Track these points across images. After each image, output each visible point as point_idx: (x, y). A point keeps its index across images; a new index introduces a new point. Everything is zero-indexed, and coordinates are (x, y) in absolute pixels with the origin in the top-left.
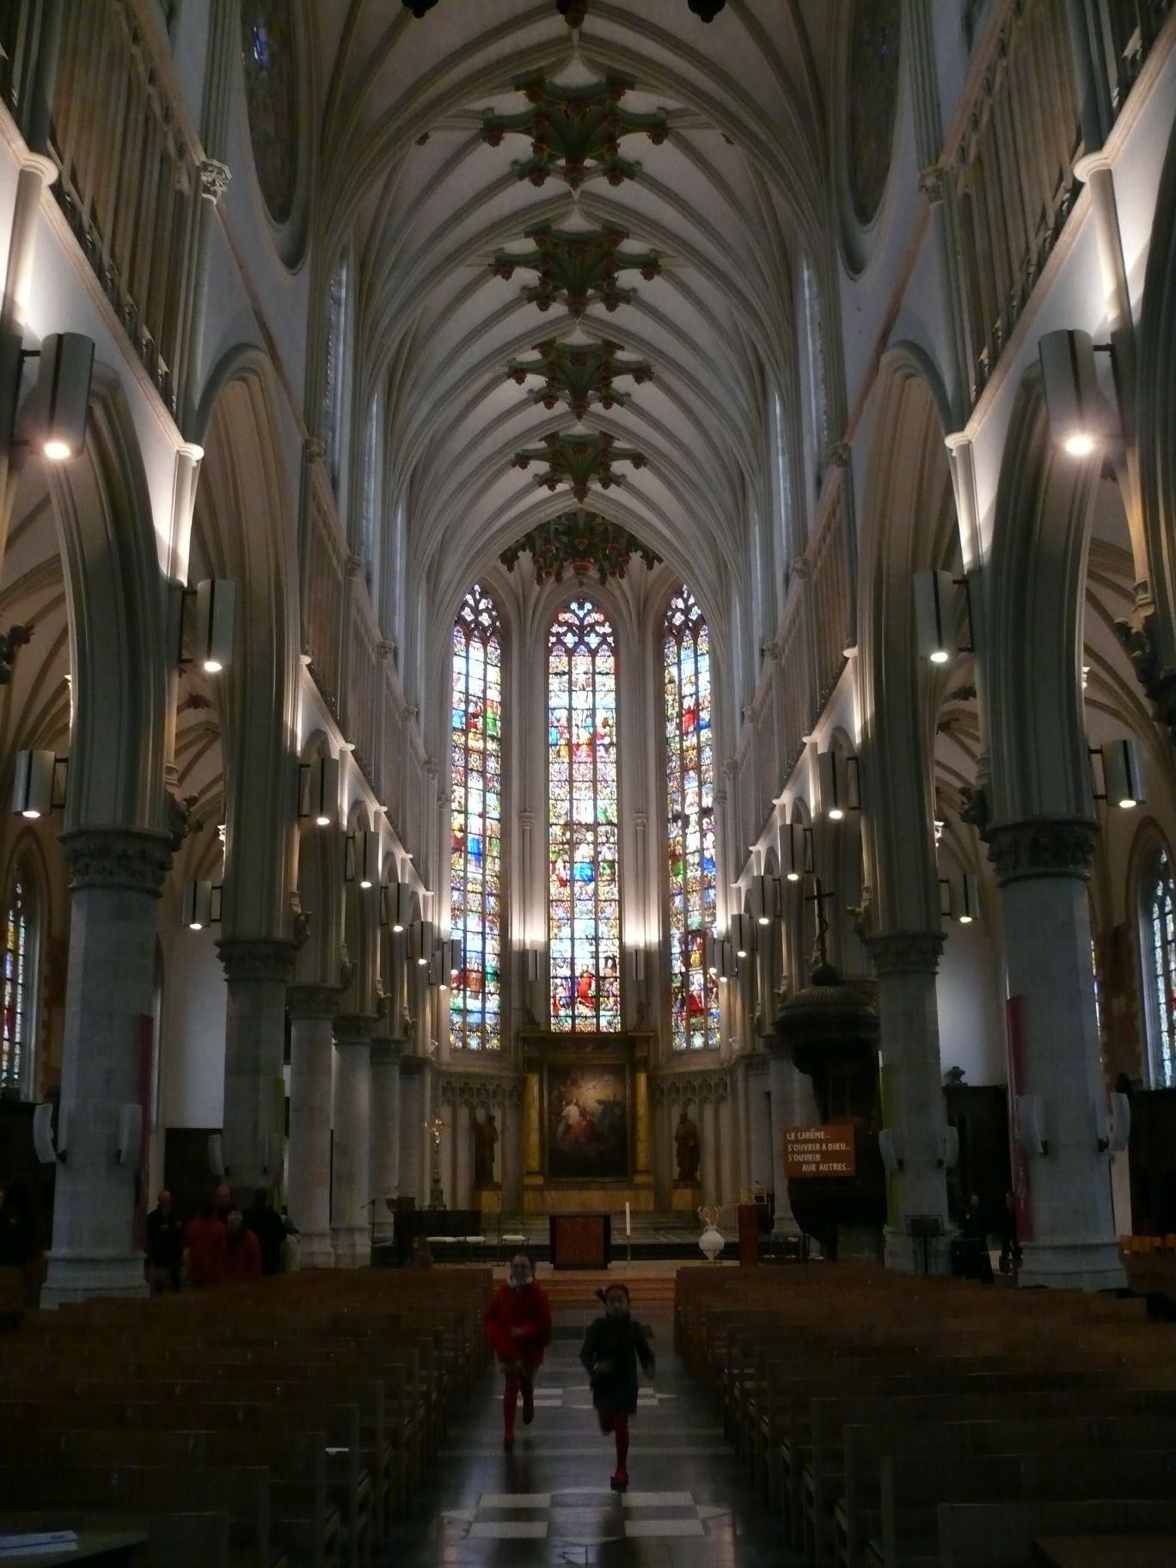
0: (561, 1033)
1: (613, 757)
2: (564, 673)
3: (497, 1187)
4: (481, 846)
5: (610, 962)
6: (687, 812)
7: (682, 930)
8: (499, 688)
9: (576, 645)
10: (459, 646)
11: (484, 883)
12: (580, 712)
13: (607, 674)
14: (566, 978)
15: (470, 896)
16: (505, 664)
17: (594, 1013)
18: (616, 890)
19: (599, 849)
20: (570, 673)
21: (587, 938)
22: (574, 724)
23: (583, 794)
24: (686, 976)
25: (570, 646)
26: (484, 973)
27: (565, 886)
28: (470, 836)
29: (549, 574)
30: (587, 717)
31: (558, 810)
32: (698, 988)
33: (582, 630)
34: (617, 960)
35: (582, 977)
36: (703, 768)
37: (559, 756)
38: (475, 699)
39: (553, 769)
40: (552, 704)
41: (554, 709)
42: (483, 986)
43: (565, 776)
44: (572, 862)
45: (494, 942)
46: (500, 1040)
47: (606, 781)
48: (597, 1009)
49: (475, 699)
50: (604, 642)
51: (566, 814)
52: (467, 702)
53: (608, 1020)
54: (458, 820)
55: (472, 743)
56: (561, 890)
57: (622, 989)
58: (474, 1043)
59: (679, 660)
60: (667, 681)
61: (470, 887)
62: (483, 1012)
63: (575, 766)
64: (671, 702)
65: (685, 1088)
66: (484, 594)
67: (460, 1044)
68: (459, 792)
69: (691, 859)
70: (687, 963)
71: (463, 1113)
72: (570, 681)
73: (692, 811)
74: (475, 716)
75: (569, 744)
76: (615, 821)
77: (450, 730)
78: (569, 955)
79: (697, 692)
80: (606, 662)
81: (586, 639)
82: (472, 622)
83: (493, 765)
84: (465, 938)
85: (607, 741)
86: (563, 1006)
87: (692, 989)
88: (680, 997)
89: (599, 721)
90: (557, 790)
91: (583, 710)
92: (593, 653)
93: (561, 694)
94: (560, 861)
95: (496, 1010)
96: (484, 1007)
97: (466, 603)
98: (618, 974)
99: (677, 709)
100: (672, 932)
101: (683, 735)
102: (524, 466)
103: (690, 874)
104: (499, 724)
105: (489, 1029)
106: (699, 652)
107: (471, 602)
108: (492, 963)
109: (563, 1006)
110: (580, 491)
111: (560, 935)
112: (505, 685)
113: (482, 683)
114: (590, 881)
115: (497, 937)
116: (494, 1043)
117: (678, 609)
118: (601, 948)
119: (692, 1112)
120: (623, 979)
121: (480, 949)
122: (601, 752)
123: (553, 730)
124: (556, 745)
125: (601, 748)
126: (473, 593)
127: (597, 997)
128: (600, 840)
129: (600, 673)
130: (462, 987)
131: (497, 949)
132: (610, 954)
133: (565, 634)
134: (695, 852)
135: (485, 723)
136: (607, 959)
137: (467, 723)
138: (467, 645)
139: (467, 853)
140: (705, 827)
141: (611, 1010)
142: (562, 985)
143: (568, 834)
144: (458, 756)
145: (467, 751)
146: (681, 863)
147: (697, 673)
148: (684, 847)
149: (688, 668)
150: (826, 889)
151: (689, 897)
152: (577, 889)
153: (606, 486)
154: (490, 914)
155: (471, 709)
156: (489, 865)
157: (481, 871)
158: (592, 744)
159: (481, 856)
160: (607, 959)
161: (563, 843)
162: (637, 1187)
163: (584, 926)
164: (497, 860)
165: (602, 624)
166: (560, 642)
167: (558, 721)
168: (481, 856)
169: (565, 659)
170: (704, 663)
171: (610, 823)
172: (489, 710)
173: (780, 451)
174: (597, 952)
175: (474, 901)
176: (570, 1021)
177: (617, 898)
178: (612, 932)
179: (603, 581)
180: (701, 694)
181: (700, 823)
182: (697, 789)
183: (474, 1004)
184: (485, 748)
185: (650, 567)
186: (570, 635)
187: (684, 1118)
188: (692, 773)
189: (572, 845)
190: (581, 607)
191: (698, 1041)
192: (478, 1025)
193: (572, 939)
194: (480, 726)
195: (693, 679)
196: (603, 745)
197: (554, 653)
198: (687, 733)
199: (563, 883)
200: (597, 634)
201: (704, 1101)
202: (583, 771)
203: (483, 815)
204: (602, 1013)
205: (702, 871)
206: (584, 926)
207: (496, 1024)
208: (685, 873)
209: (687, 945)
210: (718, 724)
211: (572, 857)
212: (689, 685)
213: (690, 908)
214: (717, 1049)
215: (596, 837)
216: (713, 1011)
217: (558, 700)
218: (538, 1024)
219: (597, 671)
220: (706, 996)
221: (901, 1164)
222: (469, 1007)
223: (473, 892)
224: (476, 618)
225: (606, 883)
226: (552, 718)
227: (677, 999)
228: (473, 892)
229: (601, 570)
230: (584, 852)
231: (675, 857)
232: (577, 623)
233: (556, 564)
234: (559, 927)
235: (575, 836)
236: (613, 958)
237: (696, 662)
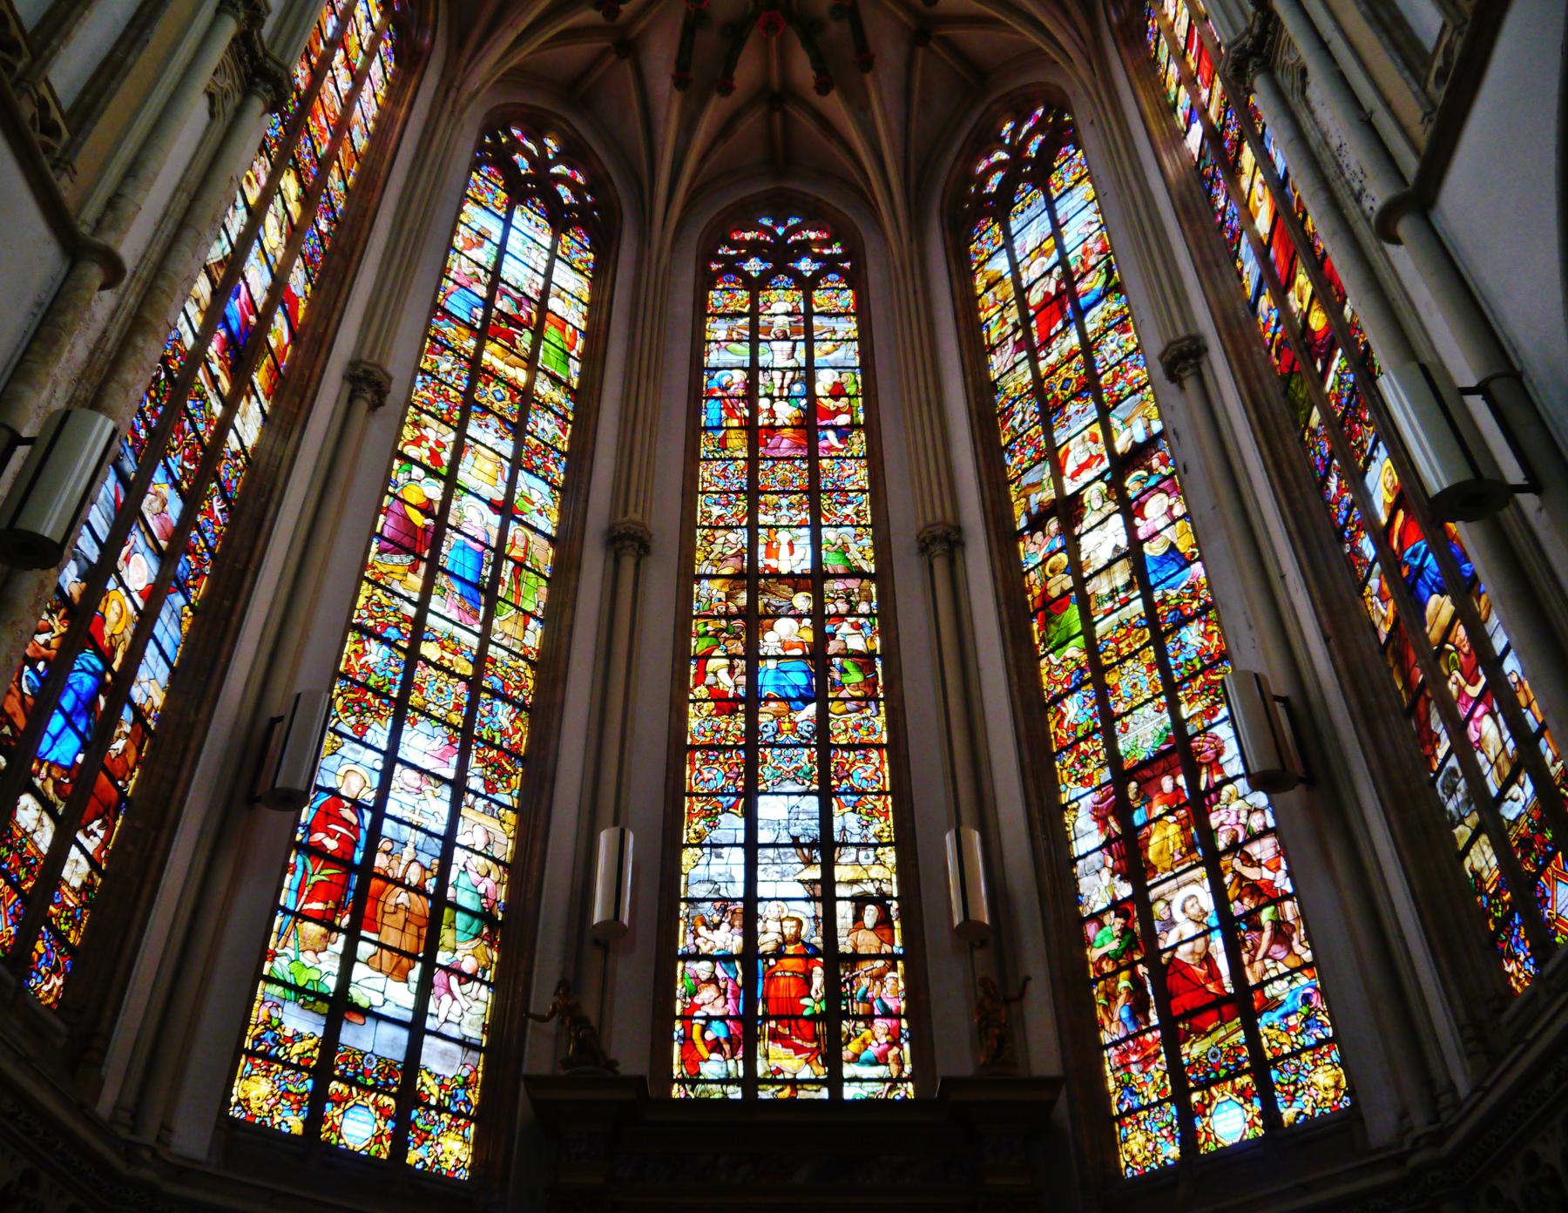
2: (741, 315)
4: (487, 572)
6: (1070, 488)
11: (481, 660)
14: (727, 959)
17: (822, 1072)
18: (880, 722)
19: (828, 629)
21: (796, 843)
26: (440, 901)
27: (733, 712)
30: (793, 382)
31: (717, 548)
32: (1190, 930)
34: (895, 905)
35: (779, 954)
37: (725, 448)
39: (707, 473)
40: (714, 358)
41: (717, 369)
42: (432, 944)
44: (753, 657)
45: (493, 824)
46: (479, 1145)
47: (844, 492)
48: (833, 1060)
51: (739, 554)
56: (722, 721)
57: (911, 994)
67: (294, 1123)
72: (754, 327)
75: (750, 426)
76: (870, 567)
78: (738, 890)
79: (1063, 255)
83: (545, 426)
85: (843, 420)
87: (1170, 939)
88: (1123, 982)
89: (821, 388)
91: (783, 370)
92: (807, 285)
93: (733, 346)
95: (474, 1033)
96: (421, 1011)
98: (898, 948)
100: (1064, 799)
103: (1100, 629)
105: (430, 1087)
109: (715, 1046)
111: (716, 836)
112: (598, 309)
113: (541, 280)
114: (806, 701)
115: (510, 817)
118: (840, 873)
120: (914, 960)
121: (439, 827)
124: (720, 428)
125: (831, 434)
127: (833, 1014)
128: (831, 609)
131: (504, 848)
132: (870, 888)
134: (1111, 563)
136: (860, 902)
139: (434, 568)
141: (880, 1060)
142: (713, 980)
143: (743, 598)
151: (1111, 679)
154: (490, 744)
155: (503, 304)
156: (505, 623)
157: (478, 628)
158: (809, 424)
159: (485, 595)
160: (860, 902)
161: (728, 616)
164: (533, 623)
167: (725, 388)
168: (485, 595)
171: (859, 574)
174: (828, 881)
178: (875, 828)
181: (1116, 488)
189: (754, 621)
192: (388, 1066)
194: (525, 339)
196: (835, 428)
200: (816, 258)
203: (506, 509)
204: (848, 1070)
207: (466, 1084)
216: (1276, 989)
220: (1233, 949)
223: (438, 667)
225: (851, 705)
226: (712, 383)
227: (1111, 997)
228: (438, 667)
230: (784, 633)
236: (881, 900)
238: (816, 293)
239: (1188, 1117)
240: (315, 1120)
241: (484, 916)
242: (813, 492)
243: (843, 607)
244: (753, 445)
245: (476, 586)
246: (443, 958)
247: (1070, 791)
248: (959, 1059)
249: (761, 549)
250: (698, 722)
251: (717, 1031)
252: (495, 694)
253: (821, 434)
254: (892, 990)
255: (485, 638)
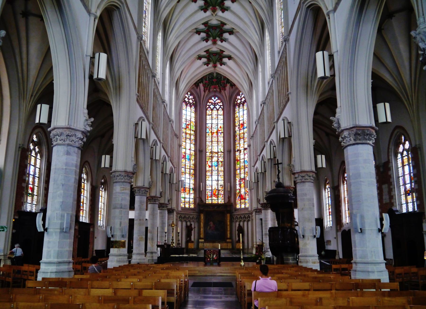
0: (209, 204)
1: (222, 136)
2: (210, 115)
3: (193, 242)
4: (189, 157)
5: (221, 186)
6: (241, 149)
7: (239, 178)
8: (194, 118)
9: (214, 108)
10: (184, 107)
11: (190, 166)
12: (214, 124)
13: (221, 115)
14: (210, 190)
15: (186, 169)
16: (196, 111)
17: (217, 199)
18: (223, 168)
20: (212, 115)
22: (213, 127)
23: (215, 144)
24: (240, 190)
25: (212, 108)
26: (190, 189)
27: (210, 167)
28: (187, 155)
29: (207, 89)
31: (209, 149)
33: (215, 104)
34: (223, 186)
35: (214, 190)
36: (245, 138)
38: (188, 121)
39: (207, 138)
40: (207, 122)
42: (190, 192)
43: (210, 140)
44: (212, 161)
47: (221, 142)
48: (218, 198)
49: (188, 121)
50: (220, 107)
51: (211, 150)
52: (186, 121)
53: (221, 201)
54: (183, 151)
55: (187, 132)
56: (209, 168)
57: (224, 193)
58: (187, 206)
59: (239, 112)
60: (236, 117)
61: (186, 167)
62: (189, 198)
63: (213, 138)
64: (237, 122)
65: (240, 218)
66: (191, 95)
68: (184, 143)
69: (241, 160)
70: (240, 187)
71: (184, 224)
73: (242, 149)
74: (188, 125)
75: (211, 132)
76: (223, 151)
77: (182, 128)
79: (243, 119)
80: (221, 112)
81: (216, 106)
82: (187, 102)
83: (193, 137)
84: (185, 180)
85: (221, 132)
86: (209, 197)
88: (238, 195)
89: (219, 127)
90: (208, 144)
94: (209, 161)
96: (190, 197)
97: (186, 97)
98: (223, 189)
99: (238, 124)
100: (237, 179)
101: (240, 130)
102: (200, 59)
103: (241, 165)
104: (194, 127)
105: (191, 202)
106: (244, 110)
107: (187, 97)
108: (192, 186)
109: (209, 197)
110: (215, 66)
111: (209, 179)
112: (196, 118)
113: (190, 117)
114: (216, 166)
115: (193, 180)
116: (192, 206)
117: (239, 99)
118: (219, 183)
119: (241, 224)
120: (224, 190)
122: (219, 134)
123: (207, 129)
125: (219, 133)
126: (187, 94)
127: (218, 195)
129: (219, 115)
130: (184, 192)
131: (193, 183)
132: (221, 184)
133: (211, 105)
135: (191, 127)
137: (186, 127)
138: (186, 107)
139: (186, 159)
140: (245, 153)
141: (221, 198)
144: (184, 135)
145: (186, 133)
146: (239, 162)
147: (243, 114)
148: (240, 158)
149: (241, 113)
150: (279, 162)
151: (241, 170)
152: (213, 168)
153: (221, 65)
155: (187, 123)
156: (191, 162)
157: (189, 163)
158: (217, 132)
160: (220, 185)
162: (227, 242)
163: (215, 177)
165: (220, 103)
166: (209, 107)
167: (209, 127)
169: (211, 111)
170: (245, 112)
171: (222, 152)
172: (192, 124)
173: (267, 50)
174: (218, 184)
175: (188, 171)
176: (211, 200)
177: (223, 170)
179: (220, 92)
180: (244, 120)
182: (243, 143)
183: (187, 196)
184: (191, 133)
185: (232, 88)
186: (212, 105)
187: (239, 224)
188: (242, 139)
190: (215, 99)
191: (243, 206)
193: (212, 180)
194: (189, 127)
195: (243, 116)
196: (220, 133)
197: (208, 110)
198: (241, 130)
199: (210, 167)
200: (219, 105)
201: (244, 221)
202: (215, 139)
203: (190, 149)
204: (219, 199)
205: (245, 163)
206: (215, 177)
208: (240, 164)
209: (240, 182)
210: (249, 127)
211: (212, 160)
212: (242, 118)
213: (241, 173)
214: (247, 208)
215: (218, 156)
217: (209, 121)
218: (203, 201)
219: (219, 114)
220: (245, 195)
221: (303, 236)
222: (186, 197)
224: (189, 101)
226: (207, 126)
229: (220, 89)
230: (215, 159)
231: (238, 160)
232: (214, 102)
233: (209, 87)
234: (209, 177)
235: (213, 155)
236: (222, 185)
237: (243, 112)
238: (219, 111)
239: (241, 205)
240: (185, 206)
241: (193, 189)
242: (218, 141)
243: (220, 156)
244: (212, 135)
245: (189, 159)
246: (190, 193)
247: (237, 179)
248: (227, 200)
249: (213, 149)
250: (208, 168)
251: (209, 196)
252: (191, 169)
253: (219, 133)
254: (222, 193)
255: (190, 164)
